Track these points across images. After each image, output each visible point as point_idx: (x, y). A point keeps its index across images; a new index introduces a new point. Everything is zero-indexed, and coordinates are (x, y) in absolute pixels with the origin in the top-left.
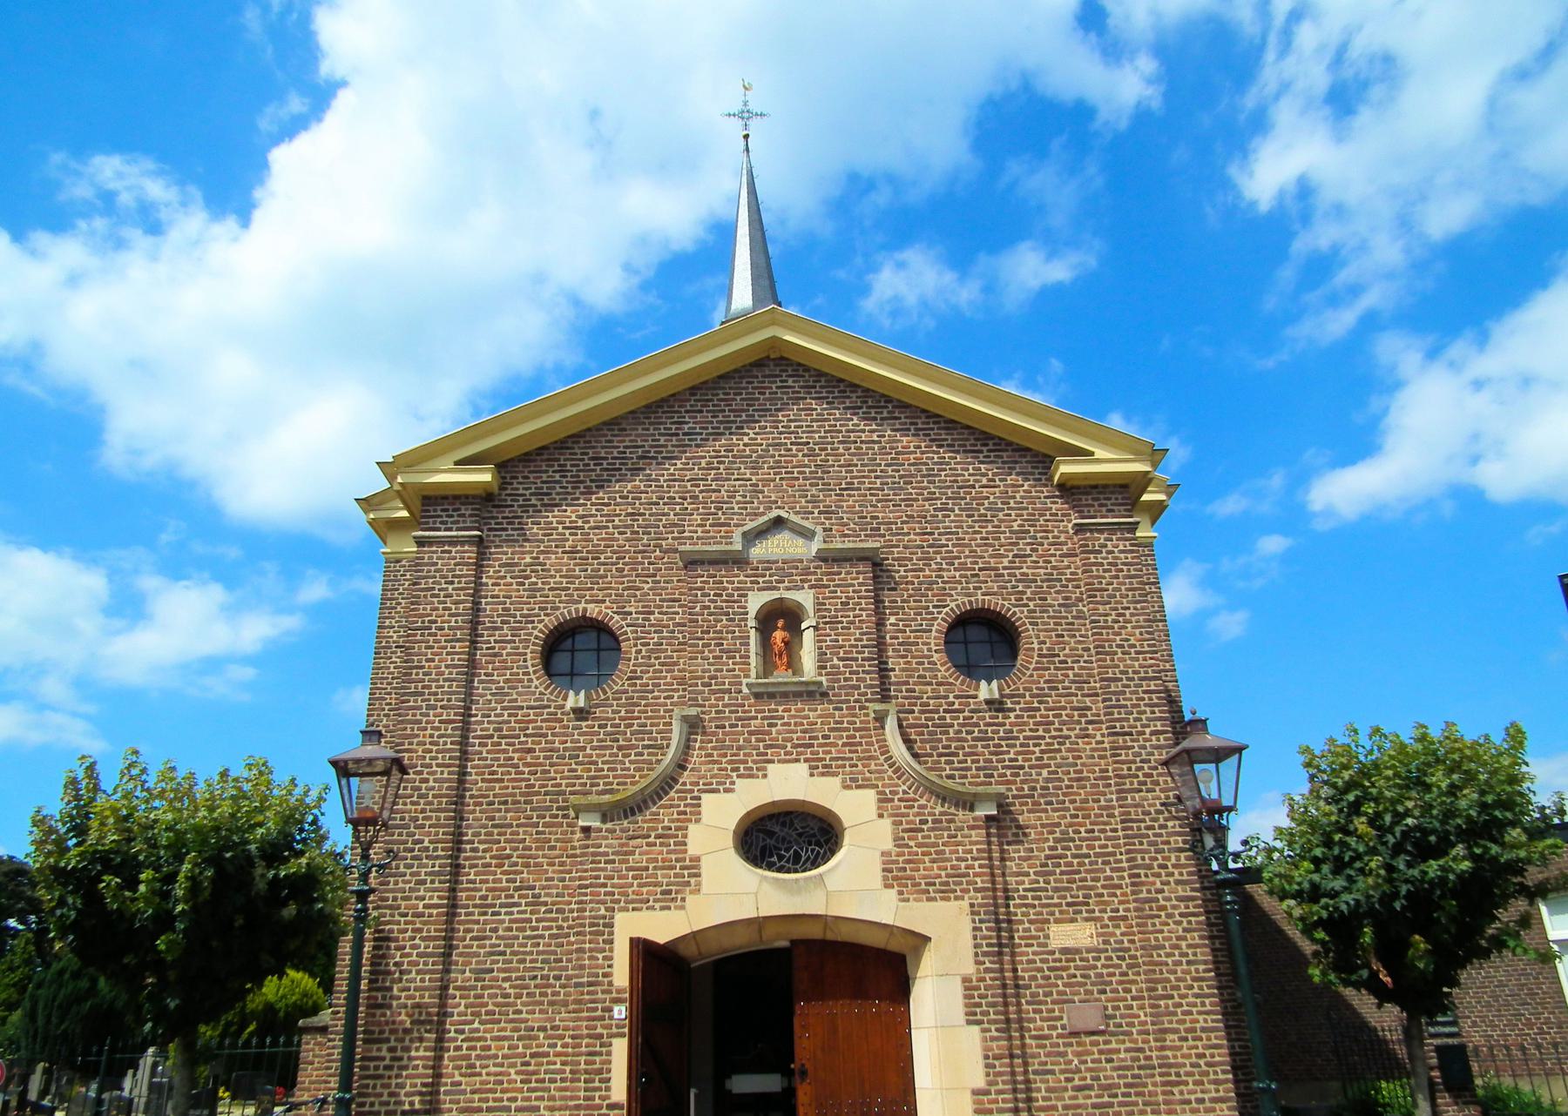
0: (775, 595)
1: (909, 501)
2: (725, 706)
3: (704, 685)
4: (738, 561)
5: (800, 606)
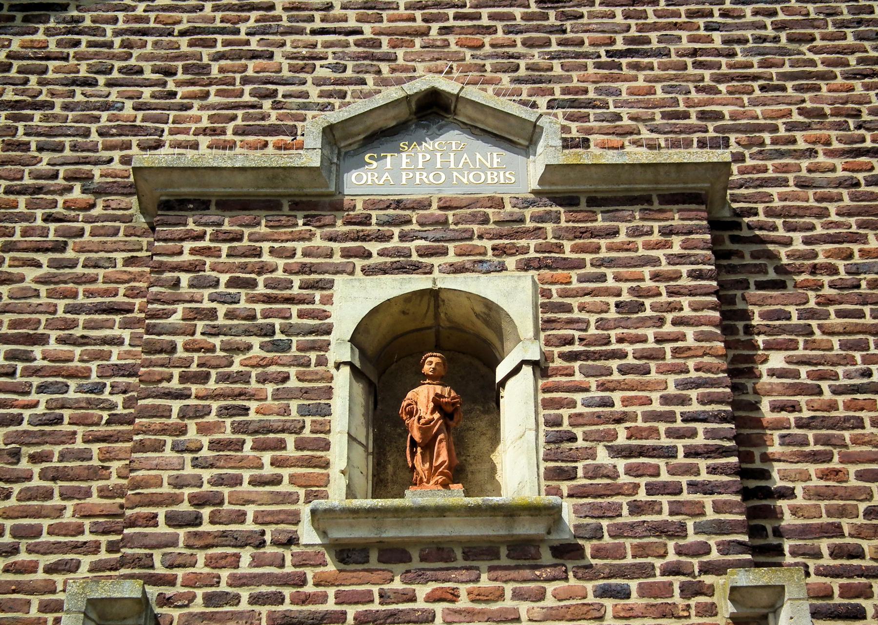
0: (418, 283)
1: (808, 79)
2: (239, 581)
3: (173, 520)
4: (310, 200)
5: (491, 314)
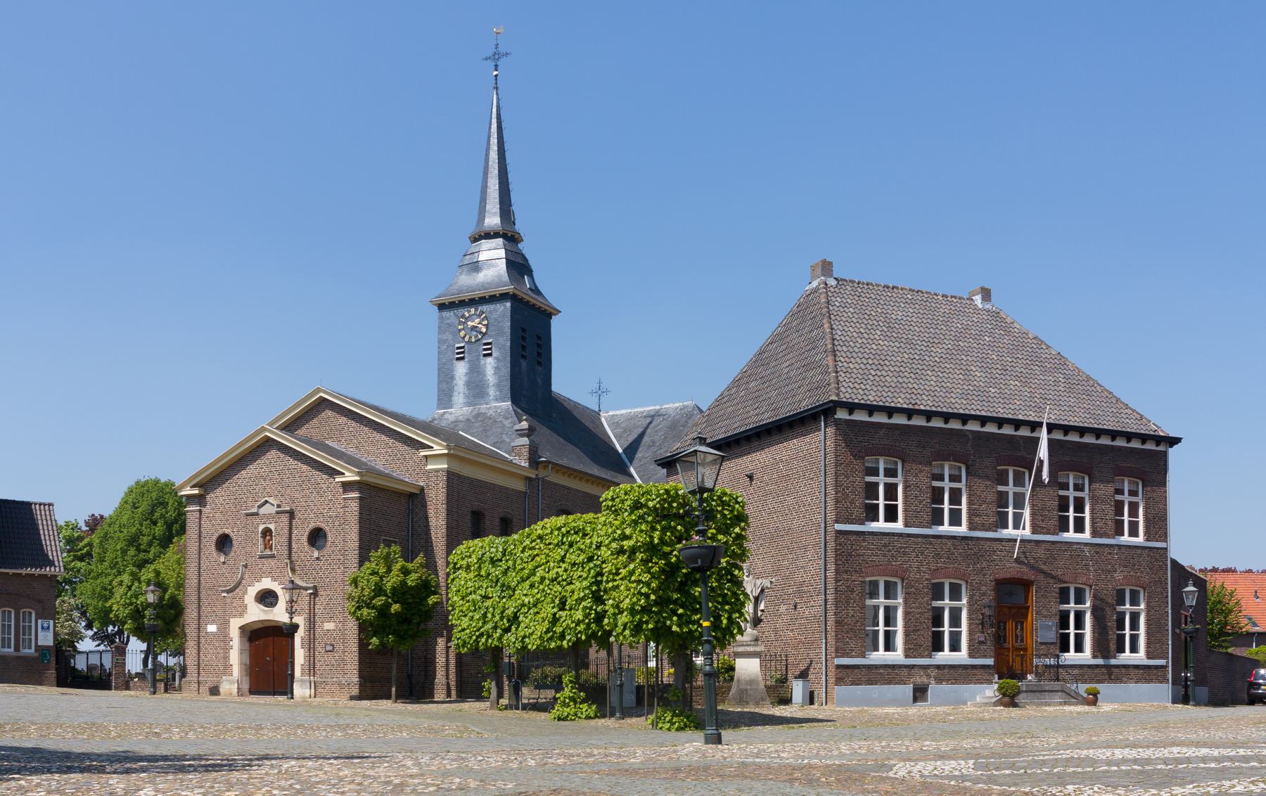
4: (257, 514)
